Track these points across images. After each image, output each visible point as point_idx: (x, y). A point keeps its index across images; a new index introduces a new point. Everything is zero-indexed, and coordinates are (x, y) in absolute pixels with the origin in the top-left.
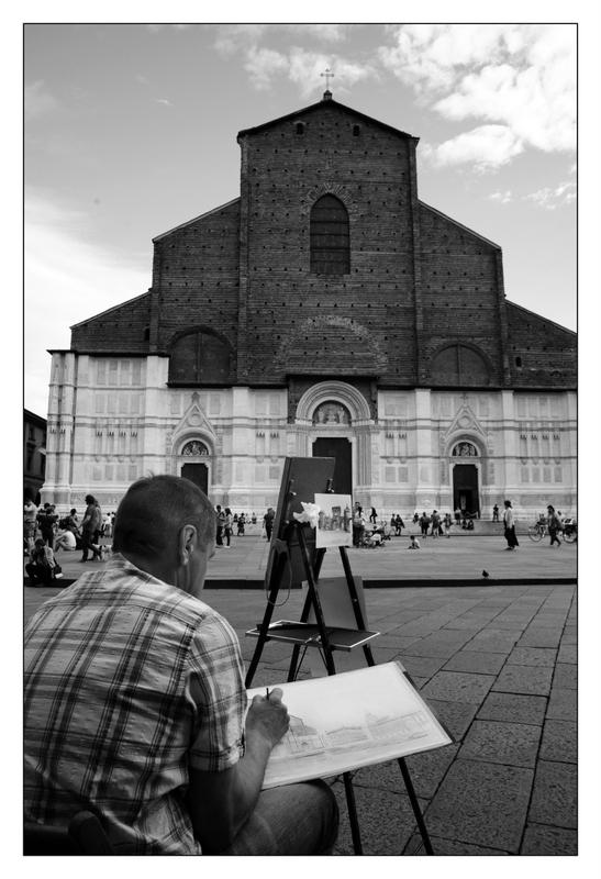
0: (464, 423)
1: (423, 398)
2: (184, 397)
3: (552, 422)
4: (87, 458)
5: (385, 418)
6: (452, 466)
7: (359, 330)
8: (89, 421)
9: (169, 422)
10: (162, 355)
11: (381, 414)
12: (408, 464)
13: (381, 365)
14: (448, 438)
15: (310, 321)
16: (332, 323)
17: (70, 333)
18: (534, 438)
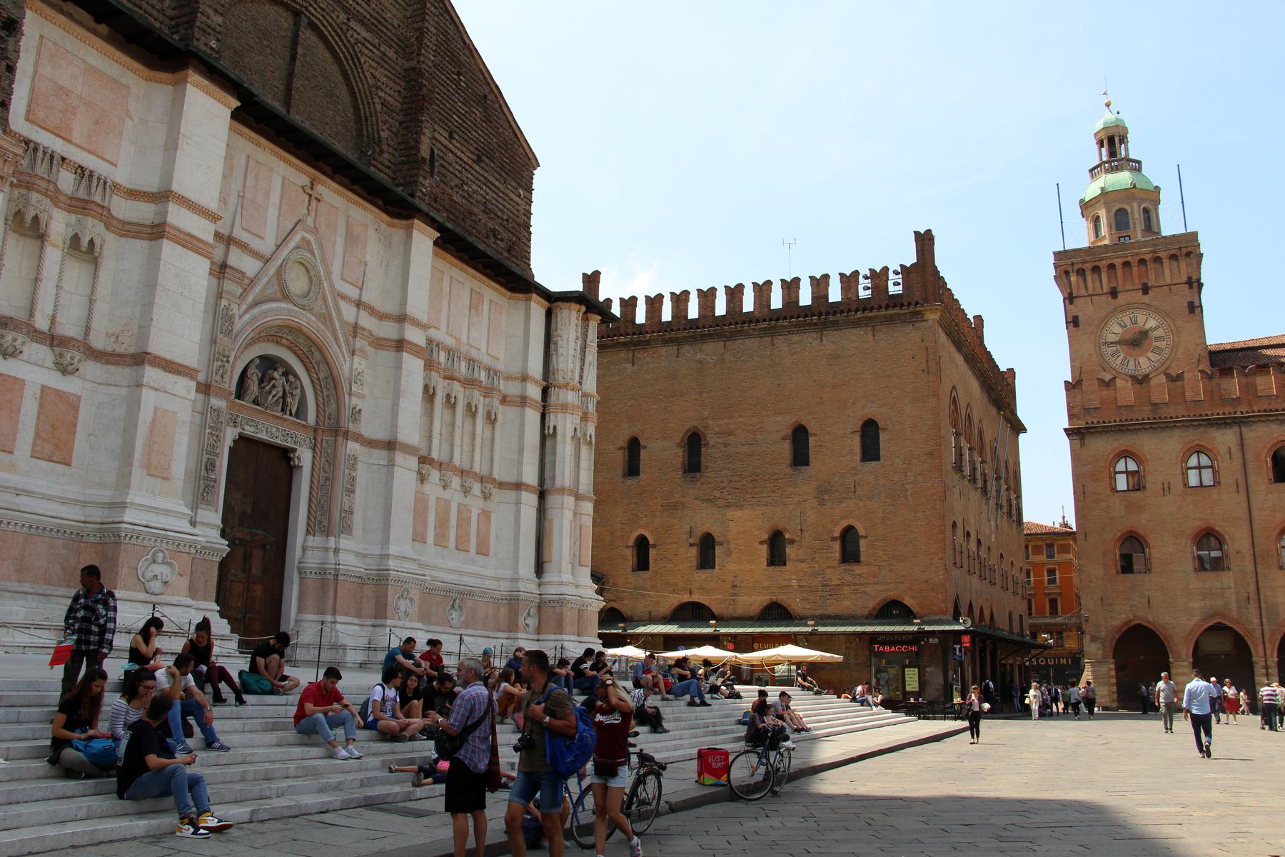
0: (297, 283)
3: (488, 370)
6: (230, 435)
12: (88, 384)
14: (245, 320)
18: (450, 402)
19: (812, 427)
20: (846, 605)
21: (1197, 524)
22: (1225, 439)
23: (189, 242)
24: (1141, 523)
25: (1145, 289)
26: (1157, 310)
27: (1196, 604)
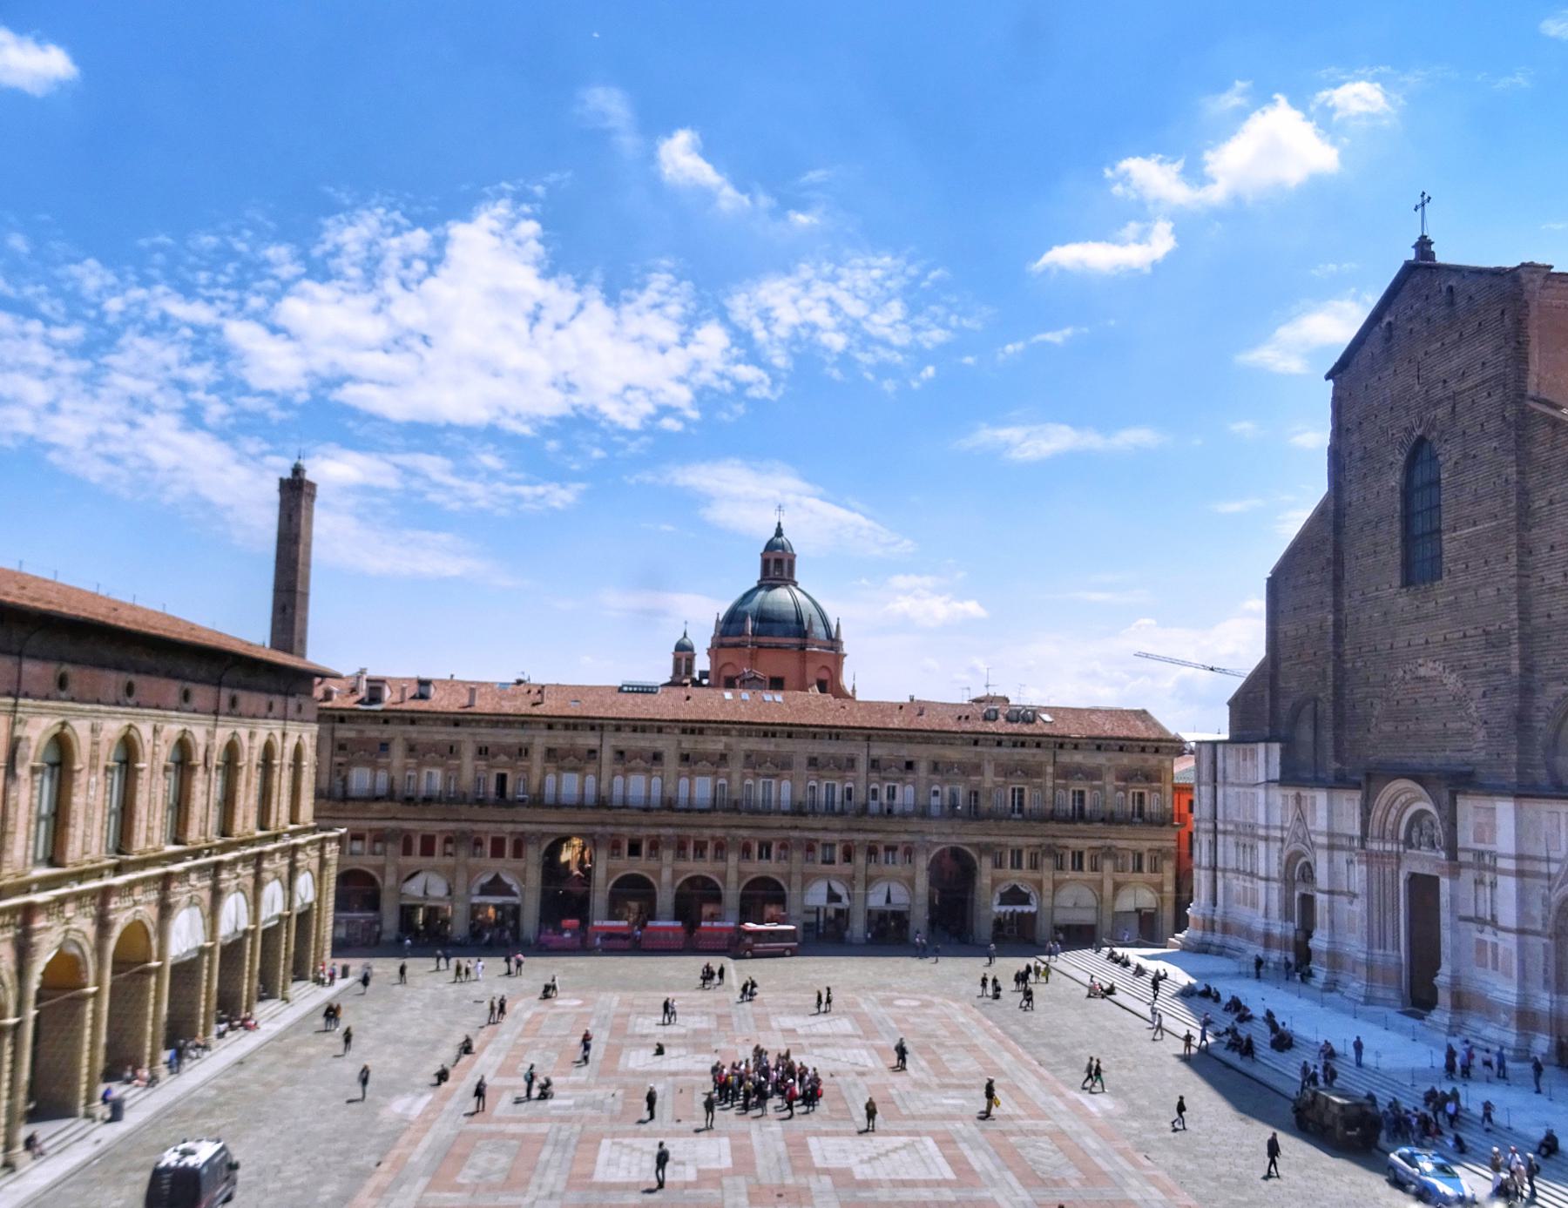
1: (1505, 809)
2: (1291, 792)
4: (1229, 875)
5: (1472, 845)
7: (1452, 680)
8: (1230, 827)
9: (1278, 834)
10: (1267, 740)
11: (1466, 838)
13: (1477, 750)
15: (1400, 673)
16: (1422, 672)
17: (1225, 712)
23: (1505, 872)
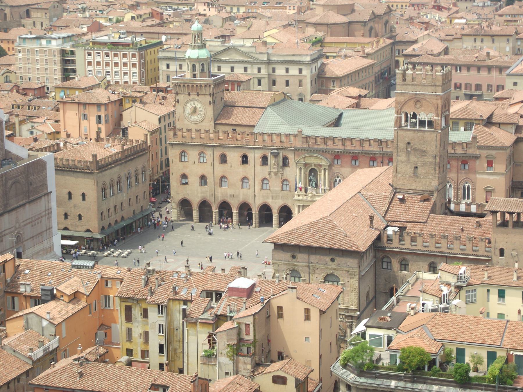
19: (72, 192)
20: (79, 229)
21: (200, 173)
22: (208, 152)
24: (187, 172)
25: (198, 95)
26: (201, 102)
27: (199, 195)
